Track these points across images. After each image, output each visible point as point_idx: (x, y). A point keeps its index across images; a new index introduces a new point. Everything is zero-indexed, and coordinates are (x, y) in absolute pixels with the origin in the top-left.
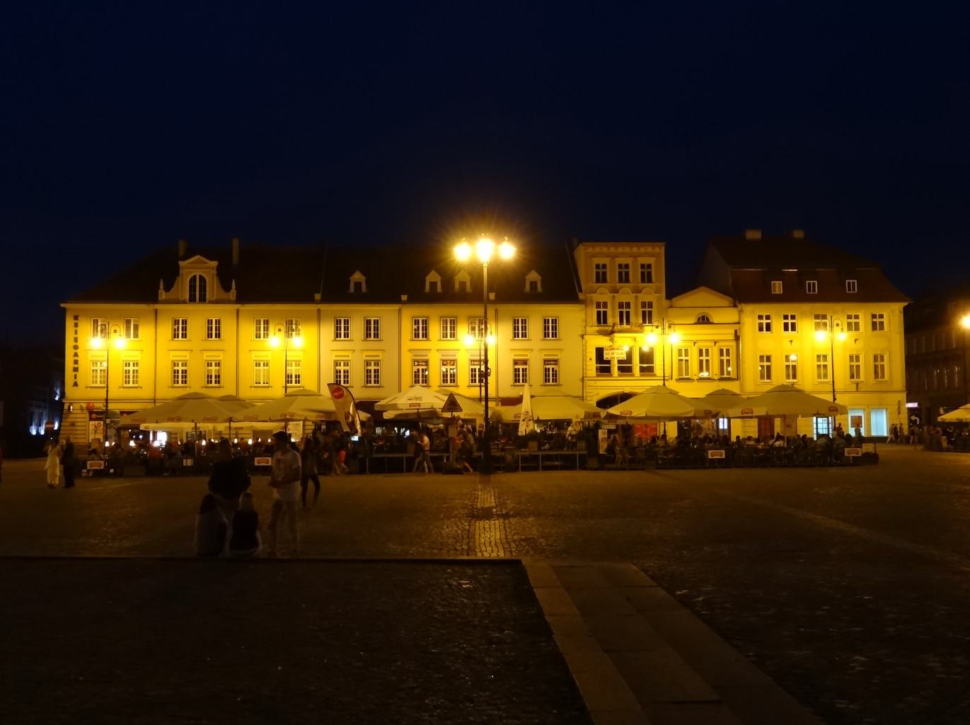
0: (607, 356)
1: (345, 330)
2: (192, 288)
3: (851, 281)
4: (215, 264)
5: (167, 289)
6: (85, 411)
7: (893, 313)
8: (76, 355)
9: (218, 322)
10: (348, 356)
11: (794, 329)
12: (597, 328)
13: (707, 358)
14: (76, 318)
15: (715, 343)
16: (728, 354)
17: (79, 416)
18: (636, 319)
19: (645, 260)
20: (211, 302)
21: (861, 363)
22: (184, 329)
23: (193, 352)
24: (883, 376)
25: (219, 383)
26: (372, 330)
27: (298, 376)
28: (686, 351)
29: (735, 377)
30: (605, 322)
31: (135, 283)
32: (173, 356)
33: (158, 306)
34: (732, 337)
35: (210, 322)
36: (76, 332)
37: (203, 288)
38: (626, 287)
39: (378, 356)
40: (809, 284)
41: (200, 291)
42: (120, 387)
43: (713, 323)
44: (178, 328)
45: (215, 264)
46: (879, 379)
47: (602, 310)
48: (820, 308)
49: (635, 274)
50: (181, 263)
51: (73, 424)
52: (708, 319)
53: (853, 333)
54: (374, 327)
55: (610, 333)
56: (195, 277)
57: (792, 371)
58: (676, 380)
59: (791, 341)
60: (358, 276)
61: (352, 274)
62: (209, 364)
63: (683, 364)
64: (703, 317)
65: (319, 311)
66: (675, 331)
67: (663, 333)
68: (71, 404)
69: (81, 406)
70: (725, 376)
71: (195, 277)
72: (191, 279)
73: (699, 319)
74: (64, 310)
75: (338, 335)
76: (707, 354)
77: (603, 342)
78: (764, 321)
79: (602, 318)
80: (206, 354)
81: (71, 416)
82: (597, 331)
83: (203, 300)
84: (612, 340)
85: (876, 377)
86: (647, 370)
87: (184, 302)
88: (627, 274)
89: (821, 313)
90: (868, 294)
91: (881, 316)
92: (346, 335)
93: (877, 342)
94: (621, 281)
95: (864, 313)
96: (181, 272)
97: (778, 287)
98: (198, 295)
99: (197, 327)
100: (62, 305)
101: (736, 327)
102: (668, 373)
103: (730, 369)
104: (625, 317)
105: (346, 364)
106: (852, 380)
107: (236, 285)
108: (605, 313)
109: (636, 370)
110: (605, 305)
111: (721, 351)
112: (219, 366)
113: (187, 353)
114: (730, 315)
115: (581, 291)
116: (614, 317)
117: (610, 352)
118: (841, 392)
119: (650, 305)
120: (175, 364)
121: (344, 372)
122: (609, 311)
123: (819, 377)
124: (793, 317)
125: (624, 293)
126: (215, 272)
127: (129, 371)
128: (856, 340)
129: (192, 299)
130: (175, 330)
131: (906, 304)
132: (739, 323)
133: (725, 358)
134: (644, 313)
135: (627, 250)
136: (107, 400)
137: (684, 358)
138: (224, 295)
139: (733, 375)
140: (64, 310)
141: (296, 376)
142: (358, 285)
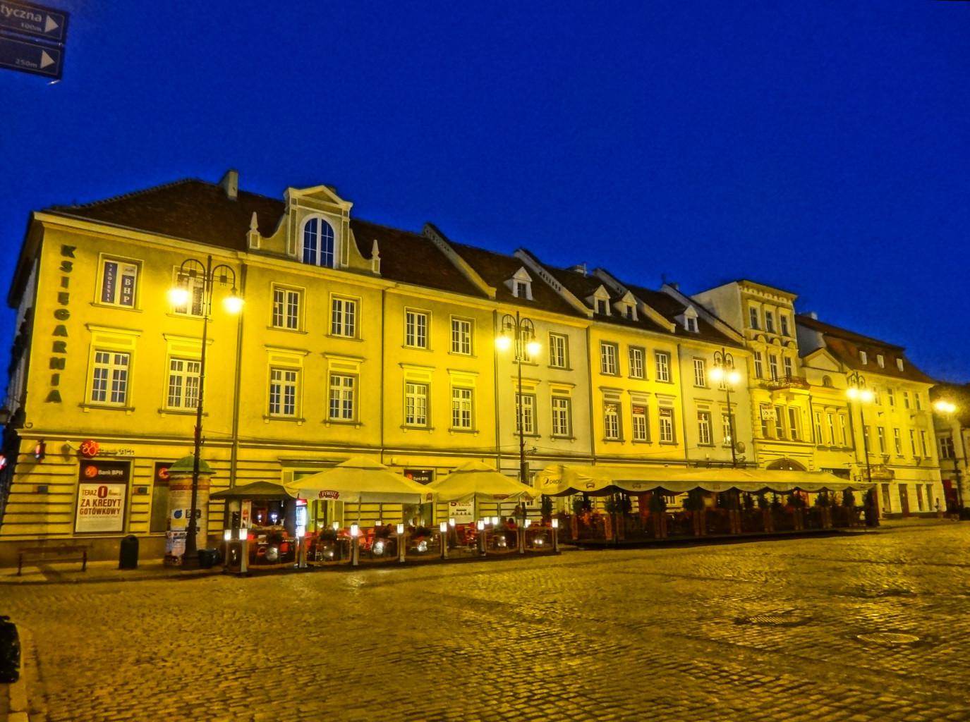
0: (766, 416)
2: (310, 241)
6: (75, 460)
8: (60, 331)
17: (55, 470)
20: (340, 269)
23: (310, 353)
25: (121, 399)
29: (851, 447)
31: (210, 212)
35: (337, 305)
36: (65, 282)
37: (328, 244)
41: (323, 248)
45: (346, 206)
59: (879, 414)
71: (314, 221)
72: (307, 228)
80: (332, 361)
87: (296, 260)
98: (318, 248)
100: (38, 216)
126: (347, 220)
127: (105, 371)
138: (360, 263)
141: (464, 412)
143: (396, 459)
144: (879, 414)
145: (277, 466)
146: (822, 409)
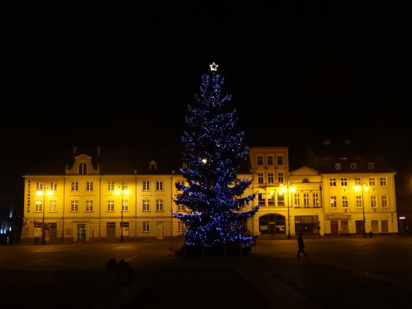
1: (147, 186)
2: (80, 168)
3: (371, 163)
4: (90, 158)
5: (69, 169)
6: (33, 223)
7: (389, 178)
8: (29, 198)
9: (92, 183)
10: (149, 198)
11: (346, 184)
12: (259, 185)
13: (308, 198)
14: (29, 182)
15: (311, 191)
16: (317, 196)
17: (30, 225)
18: (276, 181)
19: (280, 155)
20: (89, 175)
21: (376, 200)
22: (77, 186)
24: (386, 206)
25: (92, 210)
26: (159, 186)
27: (127, 207)
28: (298, 195)
29: (320, 206)
30: (262, 182)
32: (72, 198)
33: (66, 177)
34: (319, 189)
35: (88, 183)
38: (271, 167)
39: (162, 198)
40: (352, 165)
42: (48, 212)
43: (310, 183)
44: (74, 186)
45: (90, 158)
46: (385, 207)
47: (261, 177)
48: (357, 175)
49: (275, 161)
50: (76, 158)
51: (27, 229)
52: (308, 181)
53: (372, 186)
54: (160, 185)
55: (264, 187)
56: (82, 163)
57: (345, 204)
58: (294, 208)
59: (345, 190)
60: (153, 163)
61: (151, 161)
62: (88, 202)
63: (297, 201)
64: (306, 180)
65: (136, 178)
66: (293, 186)
67: (288, 187)
68: (27, 220)
69: (31, 221)
70: (316, 206)
71: (82, 163)
72: (80, 165)
73: (304, 181)
74: (24, 178)
75: (144, 189)
76: (308, 196)
77: (261, 191)
78: (333, 181)
79: (261, 181)
80: (86, 197)
81: (27, 225)
82: (259, 186)
83: (85, 173)
84: (265, 190)
85: (383, 206)
86: (281, 204)
87: (77, 175)
88: (272, 161)
89: (358, 178)
90: (379, 169)
91: (385, 179)
92: (148, 189)
93: (383, 191)
94: (269, 164)
95: (377, 178)
96: (75, 161)
97: (338, 166)
98: (83, 171)
99: (82, 186)
100: (23, 176)
101: (320, 184)
102: (290, 205)
103: (318, 202)
104: (271, 180)
105: (148, 201)
106: (373, 207)
107: (100, 167)
108: (262, 178)
109: (276, 204)
110: (262, 175)
111: (314, 195)
112: (92, 202)
113: (78, 197)
114: (318, 179)
115: (251, 168)
116: (266, 180)
117: (264, 195)
118: (366, 213)
119: (282, 174)
120: (72, 202)
121: (147, 205)
122: (264, 177)
123: (358, 206)
124: (345, 180)
125: (270, 170)
126: (90, 161)
128: (374, 190)
129: (80, 173)
130: (73, 187)
131: (395, 173)
132: (321, 182)
133: (316, 198)
134: (279, 178)
135: (272, 150)
136: (44, 218)
137: (297, 198)
138: (93, 171)
139: (319, 205)
140: (24, 178)
141: (126, 207)
142: (153, 166)
143: (104, 220)
144: (345, 190)
145: (73, 223)
146: (301, 192)
